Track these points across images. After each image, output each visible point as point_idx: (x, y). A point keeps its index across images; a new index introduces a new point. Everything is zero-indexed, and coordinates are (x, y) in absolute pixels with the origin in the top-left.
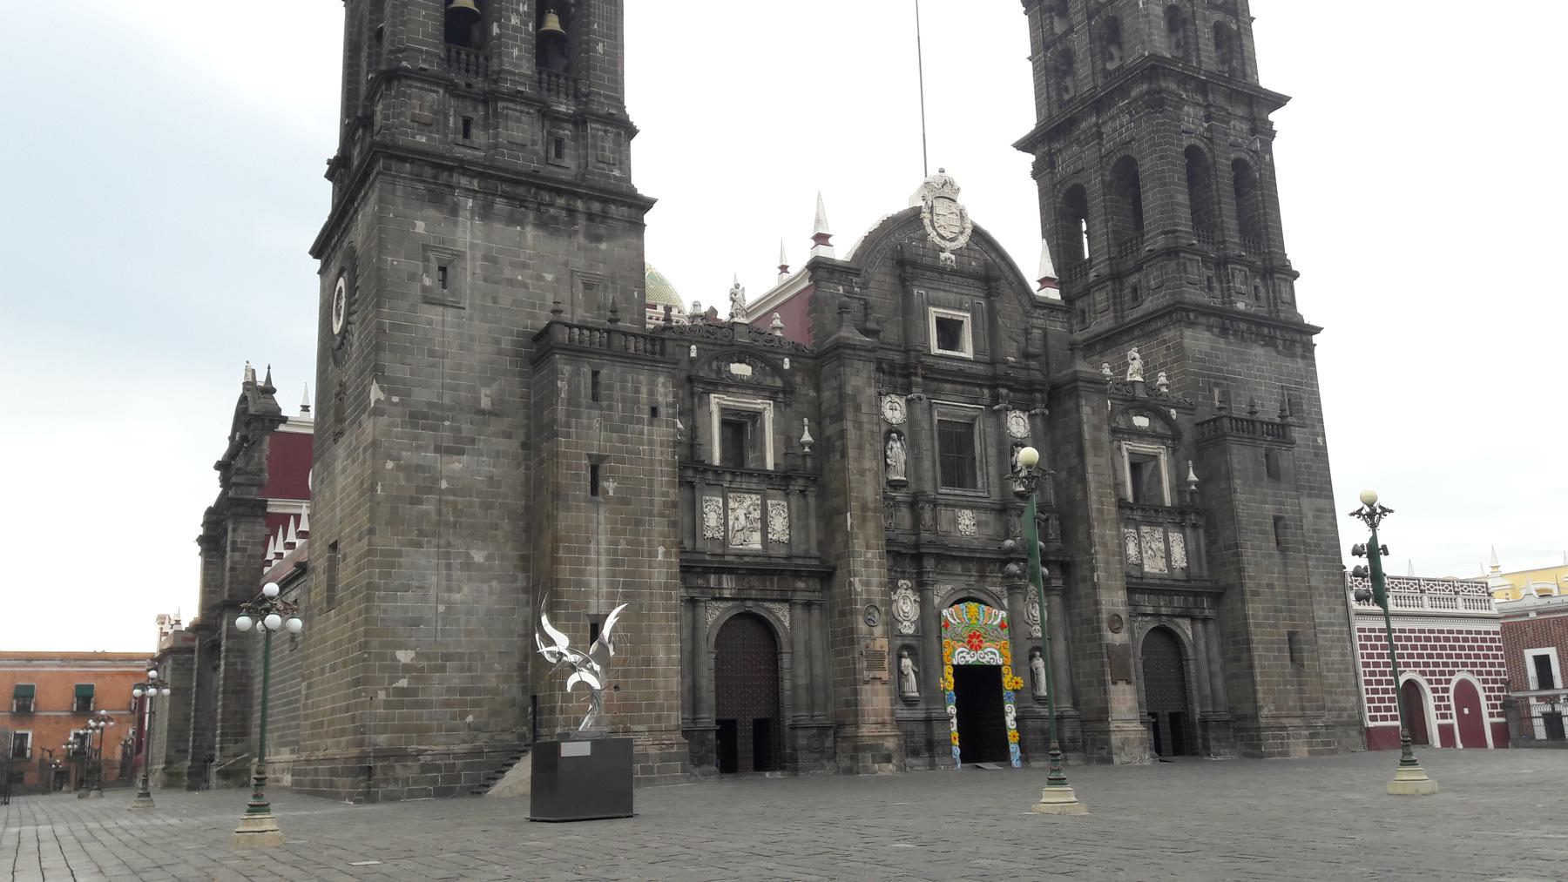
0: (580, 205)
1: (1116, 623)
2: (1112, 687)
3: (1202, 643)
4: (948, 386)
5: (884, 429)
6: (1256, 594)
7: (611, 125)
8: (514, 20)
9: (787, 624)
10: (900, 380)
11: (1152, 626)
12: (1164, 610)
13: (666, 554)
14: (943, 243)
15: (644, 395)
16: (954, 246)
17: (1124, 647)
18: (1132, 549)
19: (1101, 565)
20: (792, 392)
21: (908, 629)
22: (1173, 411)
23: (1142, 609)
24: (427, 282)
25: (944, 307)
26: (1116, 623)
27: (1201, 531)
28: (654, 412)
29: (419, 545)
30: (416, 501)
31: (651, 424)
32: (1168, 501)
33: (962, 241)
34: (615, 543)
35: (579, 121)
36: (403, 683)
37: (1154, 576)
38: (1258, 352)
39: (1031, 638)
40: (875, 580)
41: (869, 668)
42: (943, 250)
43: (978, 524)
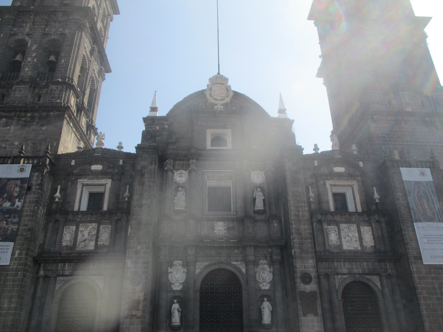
0: (37, 114)
1: (306, 279)
2: (303, 318)
7: (59, 84)
8: (29, 59)
10: (185, 162)
12: (355, 271)
13: (20, 254)
14: (216, 102)
16: (222, 102)
17: (313, 294)
18: (333, 237)
20: (123, 174)
21: (177, 287)
23: (339, 270)
25: (216, 128)
26: (306, 279)
27: (383, 225)
31: (26, 194)
33: (228, 100)
35: (47, 86)
37: (350, 251)
39: (260, 290)
42: (216, 105)
43: (228, 229)
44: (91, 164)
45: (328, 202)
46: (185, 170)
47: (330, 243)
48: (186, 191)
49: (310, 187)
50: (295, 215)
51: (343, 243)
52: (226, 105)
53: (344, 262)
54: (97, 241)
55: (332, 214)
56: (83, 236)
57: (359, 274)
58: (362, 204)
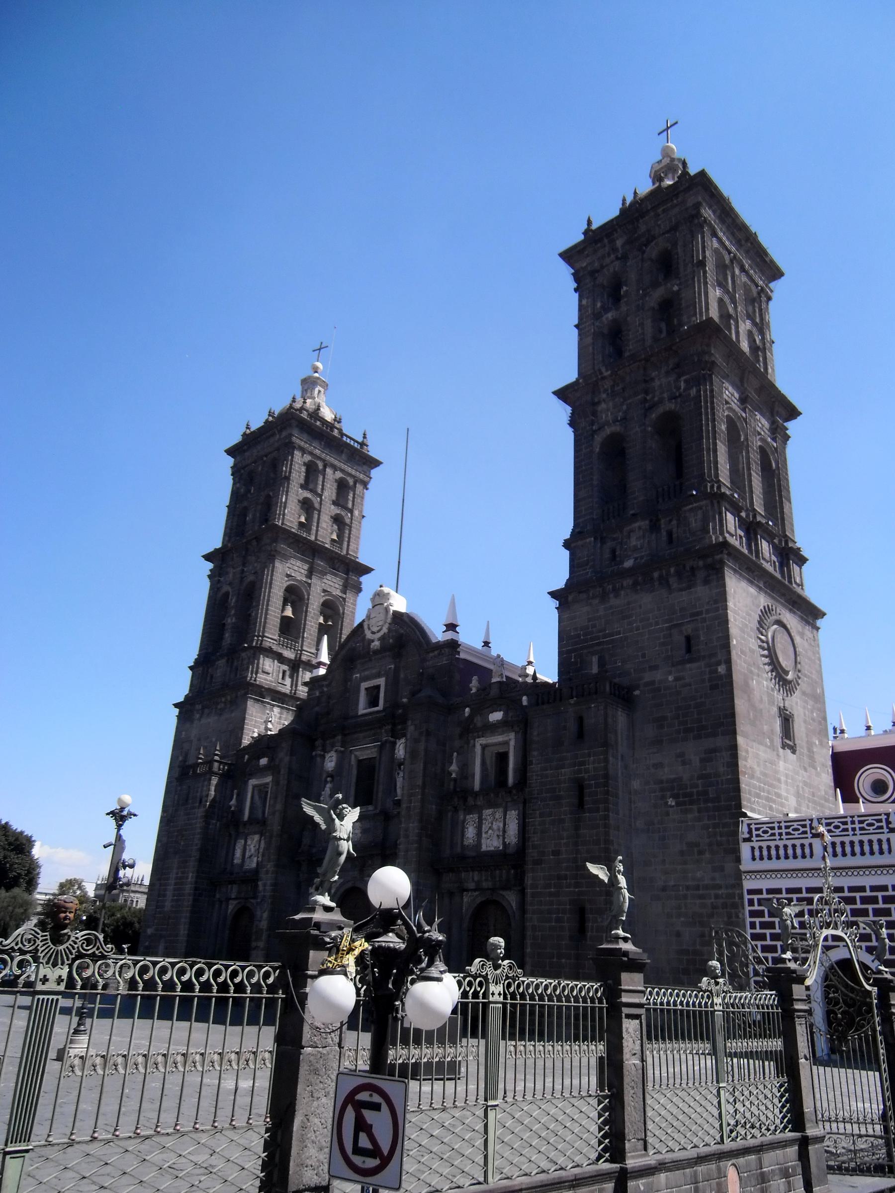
4: (361, 735)
5: (324, 776)
6: (538, 862)
8: (229, 620)
11: (479, 900)
12: (485, 885)
15: (198, 794)
18: (471, 832)
19: (402, 854)
22: (525, 698)
31: (199, 807)
32: (511, 780)
33: (385, 630)
34: (177, 874)
36: (147, 944)
38: (646, 600)
40: (269, 882)
42: (373, 641)
44: (259, 758)
45: (474, 775)
47: (466, 843)
49: (455, 754)
51: (483, 841)
52: (382, 639)
53: (473, 871)
55: (476, 795)
56: (250, 850)
57: (488, 889)
58: (515, 771)
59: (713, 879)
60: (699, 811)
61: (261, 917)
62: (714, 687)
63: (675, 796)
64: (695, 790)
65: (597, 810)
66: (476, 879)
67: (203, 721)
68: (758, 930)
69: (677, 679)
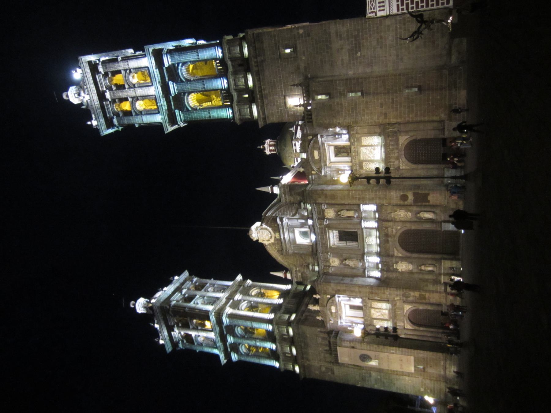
1: (404, 198)
3: (411, 134)
5: (342, 266)
9: (410, 307)
11: (404, 159)
13: (393, 350)
17: (415, 194)
21: (411, 267)
24: (330, 373)
26: (404, 198)
28: (353, 347)
29: (394, 384)
30: (384, 383)
33: (270, 229)
40: (395, 292)
41: (424, 298)
44: (331, 313)
46: (330, 259)
48: (345, 260)
50: (359, 200)
53: (390, 162)
54: (383, 309)
59: (393, 30)
60: (363, 39)
61: (413, 296)
62: (309, 36)
63: (356, 53)
64: (354, 42)
65: (362, 83)
66: (393, 160)
67: (310, 358)
68: (415, 5)
69: (304, 55)
